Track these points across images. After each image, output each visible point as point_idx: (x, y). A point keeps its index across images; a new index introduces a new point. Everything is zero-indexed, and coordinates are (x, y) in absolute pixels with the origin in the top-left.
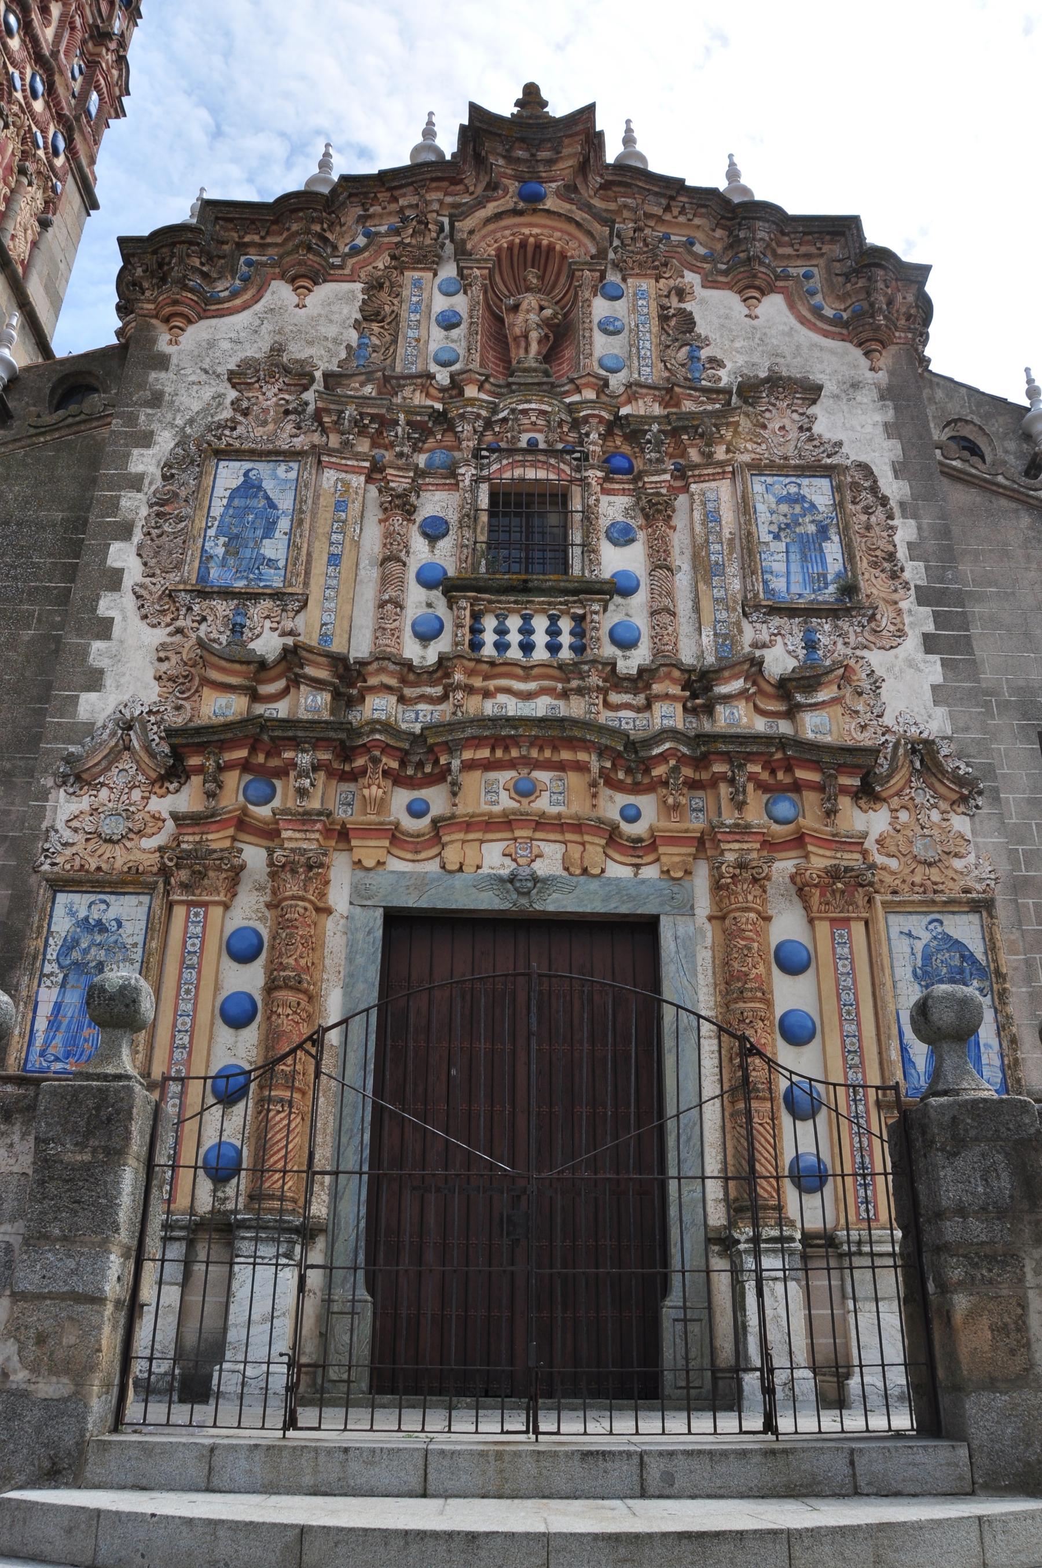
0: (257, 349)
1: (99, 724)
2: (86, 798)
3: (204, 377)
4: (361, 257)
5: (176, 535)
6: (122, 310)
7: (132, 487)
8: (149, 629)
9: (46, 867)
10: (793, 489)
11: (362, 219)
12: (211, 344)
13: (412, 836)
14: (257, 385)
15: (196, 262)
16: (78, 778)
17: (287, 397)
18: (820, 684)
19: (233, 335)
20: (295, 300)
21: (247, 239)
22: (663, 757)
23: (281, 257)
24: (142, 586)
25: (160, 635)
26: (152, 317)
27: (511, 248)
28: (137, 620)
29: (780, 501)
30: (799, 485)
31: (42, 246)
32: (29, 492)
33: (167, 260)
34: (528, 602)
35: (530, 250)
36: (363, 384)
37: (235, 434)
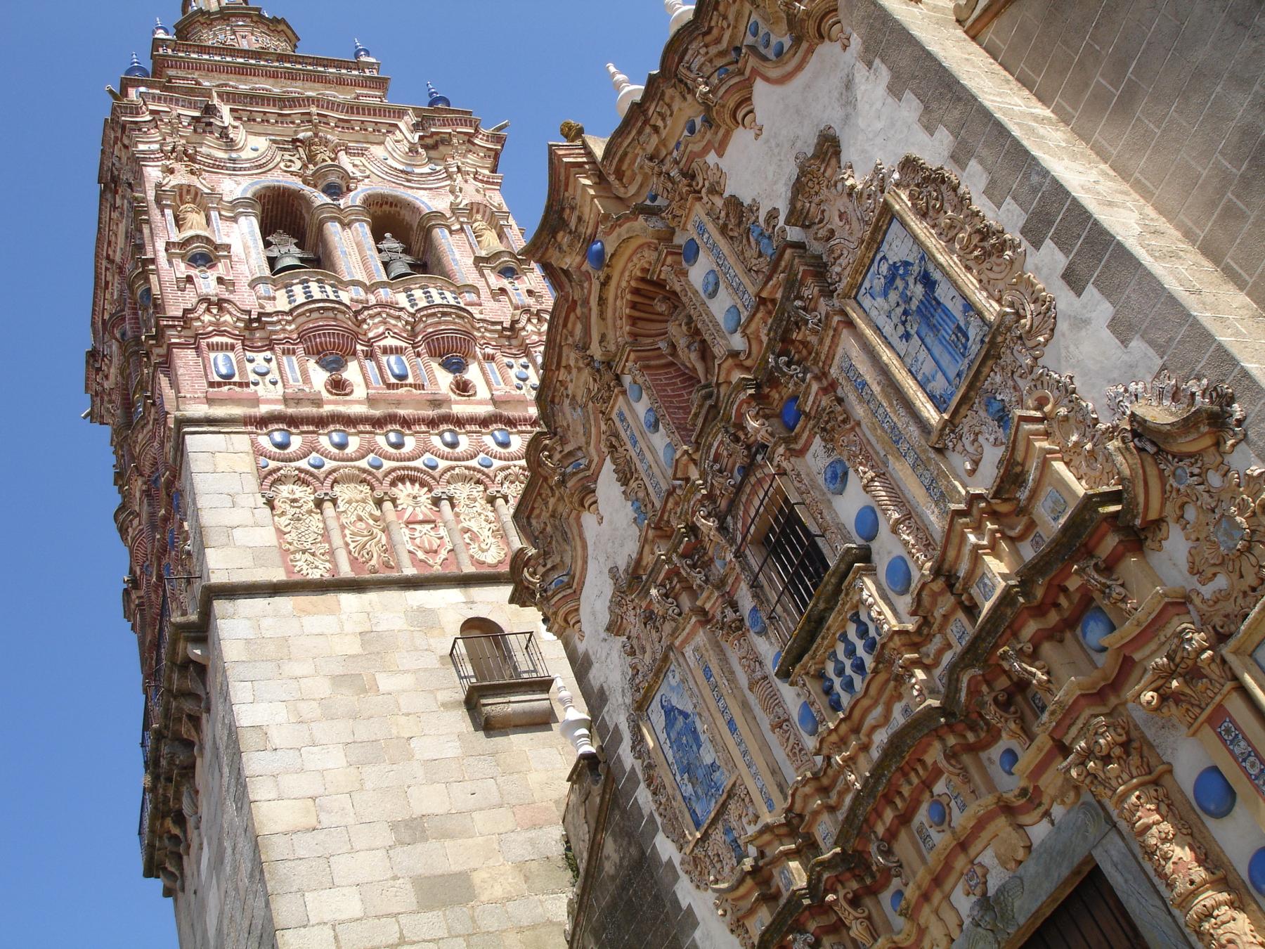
0: (609, 590)
10: (884, 268)
18: (1023, 465)
19: (596, 592)
22: (973, 691)
27: (634, 306)
29: (886, 295)
30: (884, 258)
34: (828, 629)
35: (642, 286)
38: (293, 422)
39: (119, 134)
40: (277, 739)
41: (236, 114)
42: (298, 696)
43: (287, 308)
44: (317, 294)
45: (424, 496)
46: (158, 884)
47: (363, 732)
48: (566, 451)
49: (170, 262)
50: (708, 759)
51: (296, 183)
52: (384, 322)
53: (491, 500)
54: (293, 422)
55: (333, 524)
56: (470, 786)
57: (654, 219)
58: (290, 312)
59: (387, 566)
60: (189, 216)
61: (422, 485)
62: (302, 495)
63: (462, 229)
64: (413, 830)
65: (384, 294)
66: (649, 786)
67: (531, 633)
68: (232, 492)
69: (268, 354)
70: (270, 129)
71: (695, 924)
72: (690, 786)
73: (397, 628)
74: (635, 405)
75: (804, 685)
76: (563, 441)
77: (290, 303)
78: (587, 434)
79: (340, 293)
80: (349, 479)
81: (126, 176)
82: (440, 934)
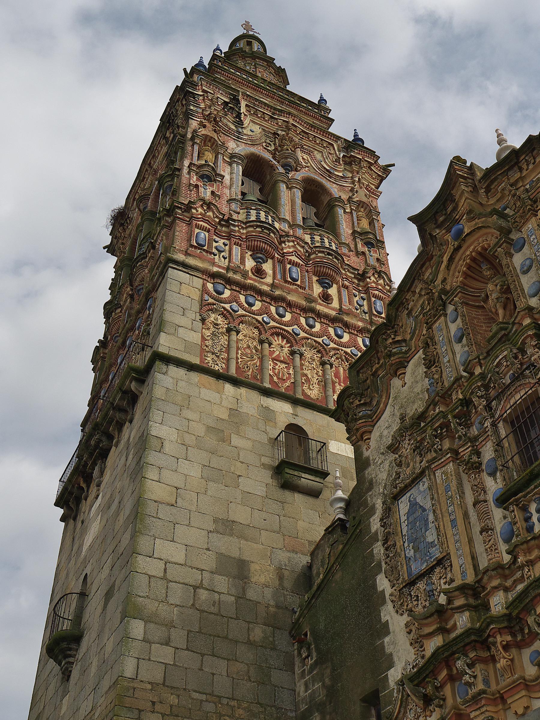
13: (534, 681)
14: (401, 445)
27: (469, 267)
35: (478, 258)
36: (435, 411)
38: (229, 282)
39: (181, 97)
40: (167, 447)
41: (248, 109)
42: (186, 430)
43: (245, 221)
44: (263, 218)
45: (286, 350)
46: (60, 512)
47: (215, 462)
48: (396, 339)
49: (189, 173)
50: (430, 539)
51: (268, 156)
52: (294, 246)
53: (323, 364)
54: (229, 282)
55: (234, 345)
56: (264, 515)
57: (502, 220)
58: (245, 223)
59: (255, 377)
60: (206, 153)
61: (288, 342)
62: (221, 323)
63: (351, 213)
64: (226, 526)
65: (299, 232)
66: (383, 545)
67: (325, 444)
68: (184, 307)
69: (227, 242)
70: (264, 123)
71: (388, 633)
72: (412, 551)
73: (251, 413)
74: (450, 324)
75: (513, 511)
76: (396, 333)
77: (246, 218)
78: (413, 334)
79: (275, 223)
80: (250, 324)
81: (179, 121)
82: (223, 591)
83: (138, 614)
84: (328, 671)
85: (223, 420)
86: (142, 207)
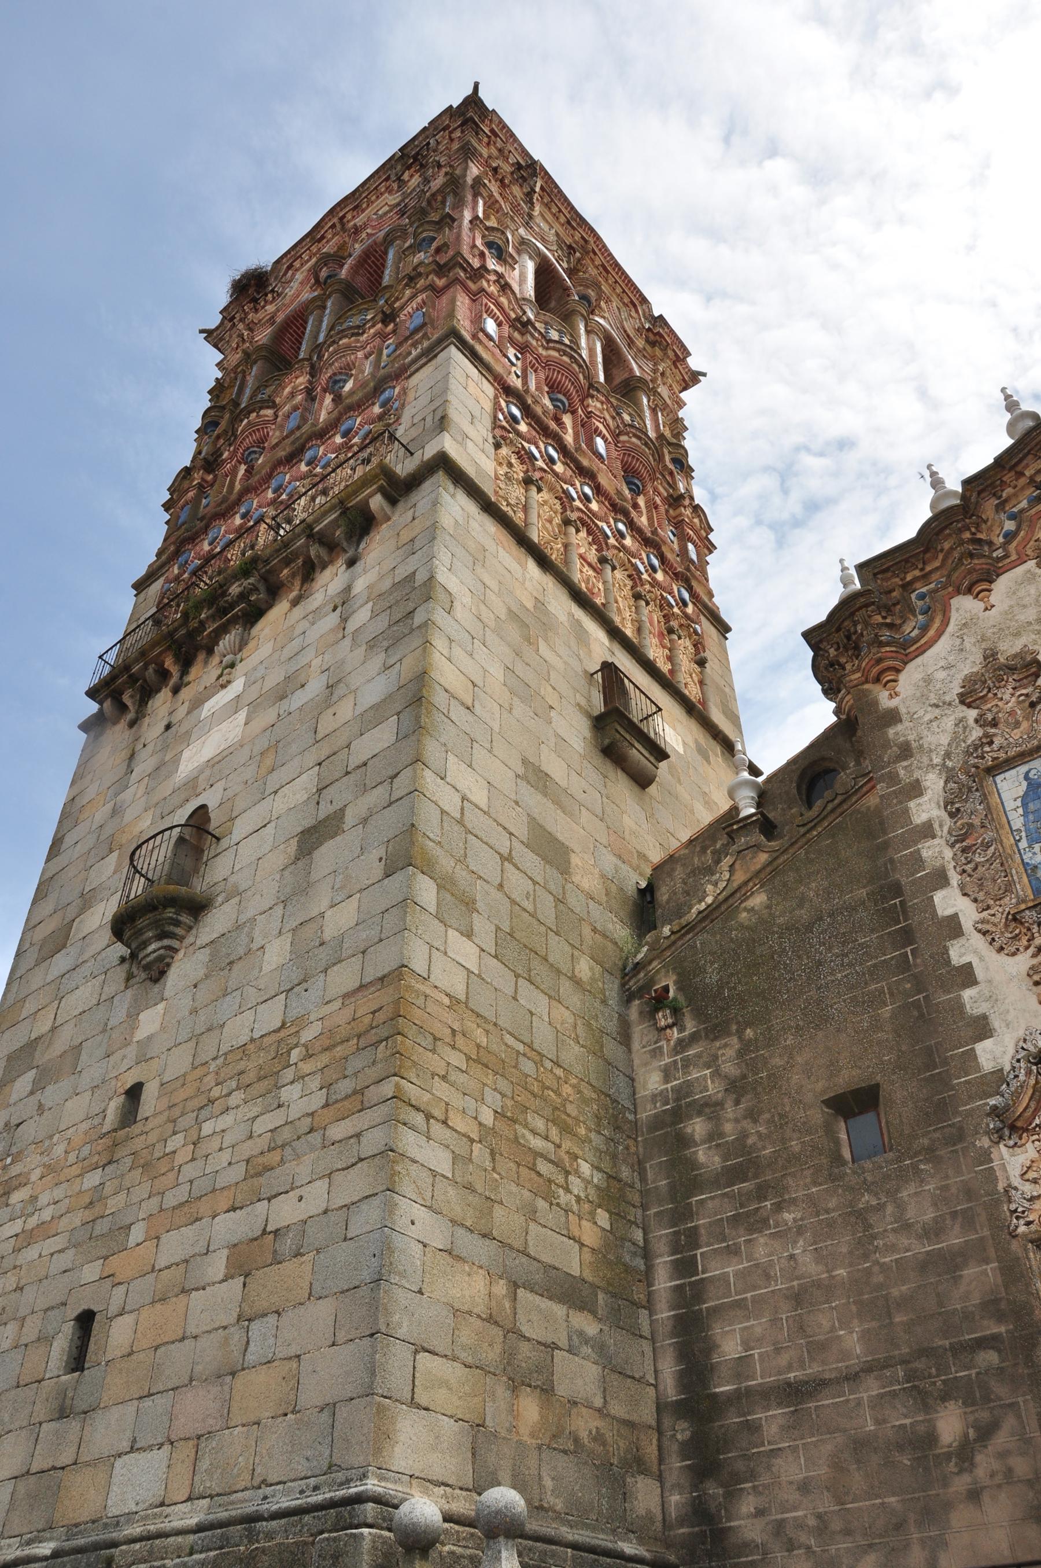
0: (971, 664)
1: (1007, 1068)
2: (1029, 1145)
3: (937, 712)
4: (1019, 538)
5: (990, 862)
6: (829, 692)
7: (925, 837)
8: (1010, 959)
9: (1022, 1229)
11: (1000, 507)
12: (928, 680)
14: (990, 695)
15: (878, 619)
16: (1013, 1128)
17: (1024, 691)
19: (942, 663)
20: (981, 605)
21: (909, 577)
23: (949, 576)
24: (983, 921)
25: (1024, 961)
26: (863, 684)
28: (994, 955)
31: (707, 681)
32: (826, 883)
33: (852, 630)
37: (995, 746)
47: (520, 668)
53: (637, 597)
64: (536, 777)
67: (660, 710)
83: (428, 868)
84: (730, 1053)
85: (527, 610)
86: (324, 273)
